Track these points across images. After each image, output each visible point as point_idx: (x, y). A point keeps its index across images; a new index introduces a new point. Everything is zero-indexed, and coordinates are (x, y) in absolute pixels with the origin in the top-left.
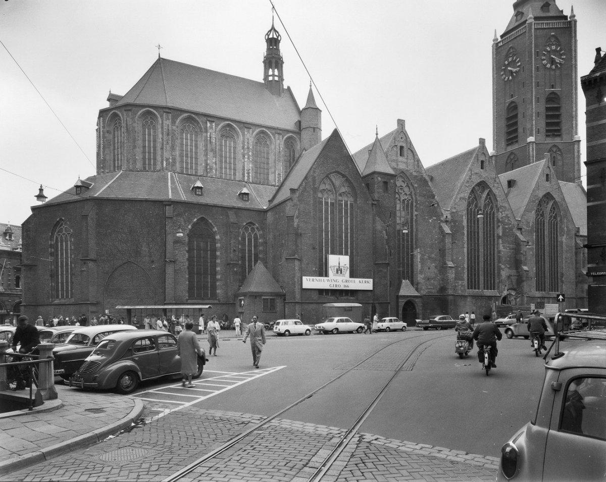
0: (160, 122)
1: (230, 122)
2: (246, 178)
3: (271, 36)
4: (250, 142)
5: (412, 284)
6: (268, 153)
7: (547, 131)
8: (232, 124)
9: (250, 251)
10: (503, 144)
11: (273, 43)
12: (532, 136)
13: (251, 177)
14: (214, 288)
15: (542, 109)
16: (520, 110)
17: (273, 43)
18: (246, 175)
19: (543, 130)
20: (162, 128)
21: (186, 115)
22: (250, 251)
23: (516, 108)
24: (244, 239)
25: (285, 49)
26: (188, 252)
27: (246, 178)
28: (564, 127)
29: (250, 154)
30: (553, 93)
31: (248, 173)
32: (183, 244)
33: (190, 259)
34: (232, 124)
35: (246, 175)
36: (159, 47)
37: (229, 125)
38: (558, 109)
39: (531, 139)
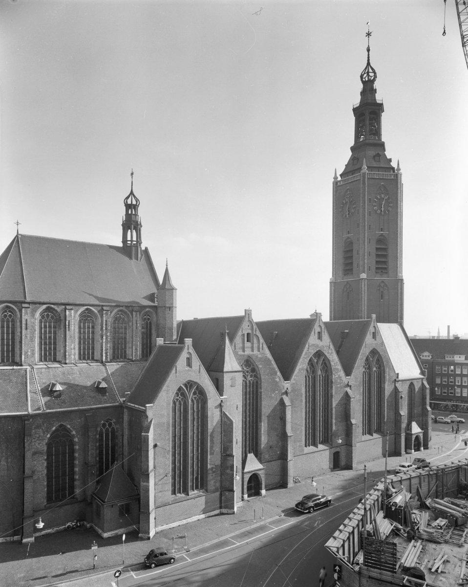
0: (19, 316)
1: (88, 307)
2: (104, 358)
3: (129, 202)
4: (109, 324)
5: (256, 456)
6: (126, 329)
7: (377, 268)
8: (91, 308)
9: (107, 445)
10: (341, 273)
11: (131, 208)
12: (364, 272)
13: (108, 357)
14: (72, 488)
15: (374, 252)
16: (355, 247)
17: (131, 208)
18: (104, 355)
19: (374, 266)
20: (21, 322)
21: (44, 307)
22: (107, 445)
23: (351, 243)
24: (101, 435)
25: (143, 215)
26: (46, 460)
27: (104, 358)
28: (391, 264)
29: (108, 334)
30: (382, 235)
31: (106, 353)
32: (42, 454)
33: (49, 468)
34: (91, 308)
35: (104, 355)
36: (18, 224)
37: (87, 309)
38: (385, 249)
39: (364, 276)
